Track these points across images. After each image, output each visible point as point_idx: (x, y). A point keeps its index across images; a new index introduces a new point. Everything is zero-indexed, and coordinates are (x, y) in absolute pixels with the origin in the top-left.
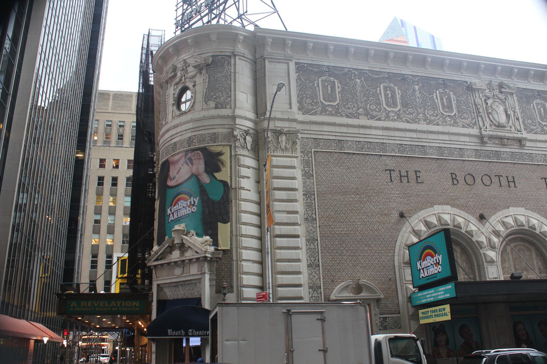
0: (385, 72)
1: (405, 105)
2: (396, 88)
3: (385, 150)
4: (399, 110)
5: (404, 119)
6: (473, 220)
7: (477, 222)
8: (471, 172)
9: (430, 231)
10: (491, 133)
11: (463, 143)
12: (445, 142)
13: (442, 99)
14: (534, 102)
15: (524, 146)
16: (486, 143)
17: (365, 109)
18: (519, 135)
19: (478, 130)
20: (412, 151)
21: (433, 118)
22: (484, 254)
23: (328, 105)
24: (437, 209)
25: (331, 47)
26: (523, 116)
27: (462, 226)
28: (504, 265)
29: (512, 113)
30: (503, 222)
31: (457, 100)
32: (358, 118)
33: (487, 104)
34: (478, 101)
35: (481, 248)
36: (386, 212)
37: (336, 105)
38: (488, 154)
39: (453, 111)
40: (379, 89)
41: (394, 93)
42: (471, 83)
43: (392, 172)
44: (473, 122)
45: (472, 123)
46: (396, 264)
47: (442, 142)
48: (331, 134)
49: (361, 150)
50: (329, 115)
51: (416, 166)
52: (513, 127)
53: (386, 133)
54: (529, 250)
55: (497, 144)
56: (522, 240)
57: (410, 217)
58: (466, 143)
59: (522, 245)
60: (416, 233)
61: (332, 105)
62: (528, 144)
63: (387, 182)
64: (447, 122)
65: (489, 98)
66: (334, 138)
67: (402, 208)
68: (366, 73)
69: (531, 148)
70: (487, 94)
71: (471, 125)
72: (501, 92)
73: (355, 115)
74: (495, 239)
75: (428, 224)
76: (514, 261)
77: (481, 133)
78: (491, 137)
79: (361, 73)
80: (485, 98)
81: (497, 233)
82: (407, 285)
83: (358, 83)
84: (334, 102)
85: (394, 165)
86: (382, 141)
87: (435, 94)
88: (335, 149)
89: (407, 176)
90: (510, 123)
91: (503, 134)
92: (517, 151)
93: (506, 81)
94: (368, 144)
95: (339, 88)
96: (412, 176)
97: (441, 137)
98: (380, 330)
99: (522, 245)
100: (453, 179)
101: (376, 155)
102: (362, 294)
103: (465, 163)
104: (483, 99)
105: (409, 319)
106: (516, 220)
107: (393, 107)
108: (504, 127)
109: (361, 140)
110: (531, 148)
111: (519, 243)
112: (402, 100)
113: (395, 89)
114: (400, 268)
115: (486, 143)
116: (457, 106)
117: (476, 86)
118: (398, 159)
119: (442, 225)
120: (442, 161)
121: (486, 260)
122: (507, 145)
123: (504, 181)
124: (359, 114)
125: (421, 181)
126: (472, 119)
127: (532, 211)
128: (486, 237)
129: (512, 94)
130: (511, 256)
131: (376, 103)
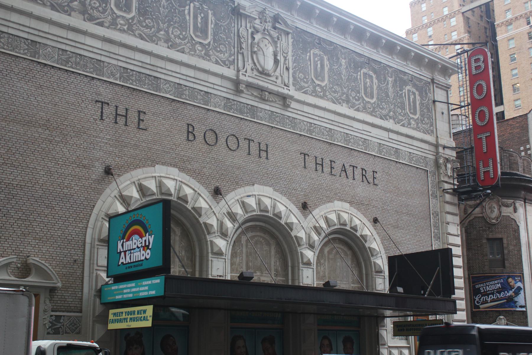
1: (143, 12)
3: (100, 72)
4: (133, 18)
5: (137, 33)
6: (205, 193)
7: (211, 197)
8: (214, 128)
9: (144, 200)
10: (250, 80)
11: (212, 86)
12: (188, 79)
13: (195, 17)
14: (312, 52)
15: (288, 106)
16: (242, 92)
18: (285, 91)
19: (235, 72)
20: (140, 81)
21: (178, 41)
22: (212, 242)
24: (160, 170)
26: (295, 67)
27: (189, 199)
28: (235, 259)
29: (282, 60)
30: (243, 203)
31: (216, 24)
32: (70, 15)
33: (253, 39)
34: (242, 30)
35: (209, 233)
36: (85, 162)
38: (242, 108)
39: (206, 37)
42: (239, 4)
43: (105, 107)
45: (229, 61)
46: (88, 240)
47: (185, 78)
48: (22, 28)
49: (64, 63)
51: (141, 104)
52: (280, 78)
53: (107, 47)
54: (269, 244)
55: (256, 97)
56: (263, 230)
57: (119, 176)
58: (216, 87)
59: (261, 237)
60: (124, 200)
62: (294, 105)
63: (95, 120)
64: (195, 51)
65: (258, 32)
66: (25, 36)
67: (110, 161)
69: (296, 111)
70: (256, 26)
71: (227, 63)
72: (275, 28)
73: (66, 8)
74: (229, 224)
75: (142, 189)
76: (247, 256)
77: (238, 76)
78: (249, 86)
81: (232, 216)
82: (99, 272)
86: (99, 57)
89: (126, 116)
90: (277, 73)
92: (278, 111)
93: (284, 14)
94: (76, 58)
96: (133, 117)
98: (48, 333)
99: (261, 237)
100: (188, 132)
101: (86, 76)
102: (29, 279)
103: (210, 113)
104: (250, 31)
105: (94, 321)
106: (259, 203)
107: (125, 11)
108: (269, 75)
111: (258, 234)
112: (139, 4)
114: (92, 247)
115: (242, 92)
117: (245, 10)
118: (117, 89)
119: (162, 194)
120: (178, 105)
121: (212, 249)
122: (267, 101)
124: (73, 9)
125: (144, 127)
128: (218, 220)
129: (287, 33)
130: (244, 250)
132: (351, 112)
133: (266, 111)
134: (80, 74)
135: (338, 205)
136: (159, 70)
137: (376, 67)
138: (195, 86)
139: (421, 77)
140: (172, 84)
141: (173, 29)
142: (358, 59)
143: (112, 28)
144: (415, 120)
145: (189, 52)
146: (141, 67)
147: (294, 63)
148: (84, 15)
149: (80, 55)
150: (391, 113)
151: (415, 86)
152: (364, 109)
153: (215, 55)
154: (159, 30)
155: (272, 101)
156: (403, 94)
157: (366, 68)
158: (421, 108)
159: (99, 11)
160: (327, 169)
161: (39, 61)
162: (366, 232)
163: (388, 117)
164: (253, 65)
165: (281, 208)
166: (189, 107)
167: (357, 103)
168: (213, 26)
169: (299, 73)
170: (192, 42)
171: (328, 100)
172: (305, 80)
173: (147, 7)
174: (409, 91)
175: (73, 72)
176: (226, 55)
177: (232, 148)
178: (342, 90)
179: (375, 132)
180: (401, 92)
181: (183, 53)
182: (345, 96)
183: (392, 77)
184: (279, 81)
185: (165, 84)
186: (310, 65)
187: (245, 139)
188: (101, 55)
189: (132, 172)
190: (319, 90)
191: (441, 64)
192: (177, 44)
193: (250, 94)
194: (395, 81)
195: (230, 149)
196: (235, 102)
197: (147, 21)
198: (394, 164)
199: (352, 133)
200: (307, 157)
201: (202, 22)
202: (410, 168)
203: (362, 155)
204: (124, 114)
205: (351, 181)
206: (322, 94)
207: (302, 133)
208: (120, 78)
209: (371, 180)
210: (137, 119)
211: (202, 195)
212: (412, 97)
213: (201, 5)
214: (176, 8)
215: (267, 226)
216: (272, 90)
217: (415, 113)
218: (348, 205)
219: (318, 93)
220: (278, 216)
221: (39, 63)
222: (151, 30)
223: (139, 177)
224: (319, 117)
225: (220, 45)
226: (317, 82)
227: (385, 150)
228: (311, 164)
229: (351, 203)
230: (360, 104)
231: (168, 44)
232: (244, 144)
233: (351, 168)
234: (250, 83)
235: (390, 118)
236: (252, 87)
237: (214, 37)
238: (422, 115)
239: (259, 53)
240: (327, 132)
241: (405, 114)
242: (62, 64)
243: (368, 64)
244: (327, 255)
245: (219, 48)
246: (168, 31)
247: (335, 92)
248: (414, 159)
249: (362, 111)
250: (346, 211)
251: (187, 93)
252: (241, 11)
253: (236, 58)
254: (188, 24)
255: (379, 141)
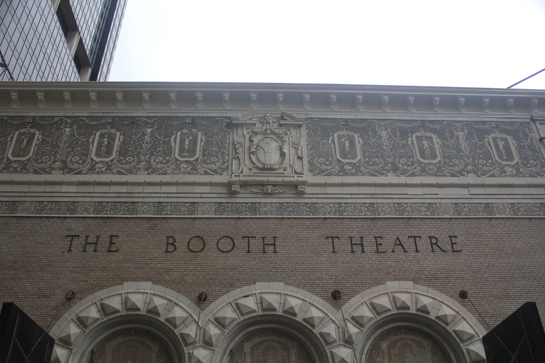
0: (109, 117)
1: (123, 152)
2: (118, 133)
4: (112, 161)
5: (115, 171)
7: (193, 305)
9: (105, 319)
11: (199, 195)
12: (170, 195)
13: (182, 141)
15: (303, 193)
17: (64, 162)
18: (296, 178)
21: (159, 166)
23: (16, 161)
25: (38, 94)
26: (313, 154)
30: (237, 305)
31: (207, 142)
32: (50, 174)
33: (251, 141)
37: (26, 160)
39: (194, 154)
40: (93, 136)
41: (113, 140)
44: (223, 167)
47: (166, 195)
48: (5, 194)
50: (11, 172)
55: (257, 193)
58: (203, 195)
61: (19, 161)
62: (308, 190)
63: (63, 252)
64: (180, 169)
66: (7, 199)
68: (83, 120)
69: (316, 196)
72: (281, 125)
73: (47, 170)
75: (104, 309)
78: (244, 185)
79: (76, 120)
80: (251, 134)
83: (67, 132)
84: (24, 156)
85: (81, 229)
86: (73, 200)
87: (174, 136)
88: (5, 213)
89: (96, 243)
91: (265, 179)
95: (38, 139)
96: (105, 242)
97: (165, 189)
100: (168, 244)
101: (59, 217)
104: (247, 136)
107: (105, 157)
108: (275, 169)
109: (45, 199)
110: (316, 196)
111: (270, 338)
112: (121, 148)
113: (115, 135)
116: (204, 149)
117: (238, 120)
118: (89, 221)
119: (128, 310)
120: (157, 221)
123: (256, 245)
125: (116, 249)
126: (224, 163)
127: (298, 286)
129: (300, 126)
131: (82, 154)
132: (403, 180)
133: (273, 205)
134: (53, 217)
135: (392, 285)
136: (136, 195)
137: (436, 127)
138: (179, 200)
139: (512, 120)
140: (151, 204)
141: (155, 157)
142: (406, 126)
143: (89, 174)
144: (513, 166)
145: (172, 172)
146: (117, 197)
147: (310, 150)
148: (63, 170)
149: (55, 202)
150: (469, 167)
151: (503, 131)
152: (424, 172)
153: (204, 167)
154: (139, 162)
155: (279, 193)
156: (486, 144)
157: (419, 132)
158: (519, 152)
159: (79, 164)
160: (370, 248)
161: (15, 215)
162: (446, 311)
163: (464, 173)
164: (252, 165)
165: (294, 302)
166: (170, 221)
167: (409, 168)
168: (202, 144)
169: (318, 159)
170: (177, 163)
171: (364, 174)
172: (327, 163)
173: (129, 147)
174: (494, 139)
175: (47, 217)
176: (218, 164)
177: (225, 250)
178: (385, 160)
179: (443, 192)
180: (481, 143)
181: (165, 174)
182: (389, 165)
183: (463, 131)
184: (289, 172)
185: (143, 206)
186: (335, 147)
187: (243, 237)
188: (76, 197)
189: (95, 294)
190: (349, 168)
191: (536, 98)
192: (158, 169)
193: (249, 192)
194: (470, 133)
195: (223, 252)
196: (230, 204)
197: (127, 159)
198: (486, 221)
199: (407, 201)
200: (336, 240)
201: (189, 144)
202: (515, 222)
203: (428, 222)
204: (95, 242)
205: (413, 254)
206: (353, 171)
207: (327, 216)
208: (94, 212)
209: (449, 247)
210: (108, 243)
211: (180, 304)
212: (501, 144)
213: (190, 130)
214: (161, 140)
215: (281, 327)
216: (275, 181)
217: (511, 158)
218: (411, 283)
219: (347, 171)
220: (291, 312)
221: (16, 217)
222: (130, 164)
223: (102, 297)
224: (351, 194)
225: (210, 157)
226: (345, 161)
227: (466, 210)
228: (343, 246)
229: (416, 280)
230: (415, 168)
231: (148, 171)
232: (241, 244)
233: (412, 240)
234: (245, 182)
235: (468, 172)
236: (250, 185)
237: (203, 152)
238: (525, 159)
239: (258, 151)
240: (367, 208)
241: (492, 164)
242: (36, 213)
243: (423, 127)
244: (386, 351)
245: (210, 160)
246: (149, 161)
247: (374, 164)
248: (522, 209)
249: (420, 175)
250: (406, 290)
251: (169, 208)
252: (234, 122)
253: (230, 164)
254: (173, 149)
255: (454, 201)
